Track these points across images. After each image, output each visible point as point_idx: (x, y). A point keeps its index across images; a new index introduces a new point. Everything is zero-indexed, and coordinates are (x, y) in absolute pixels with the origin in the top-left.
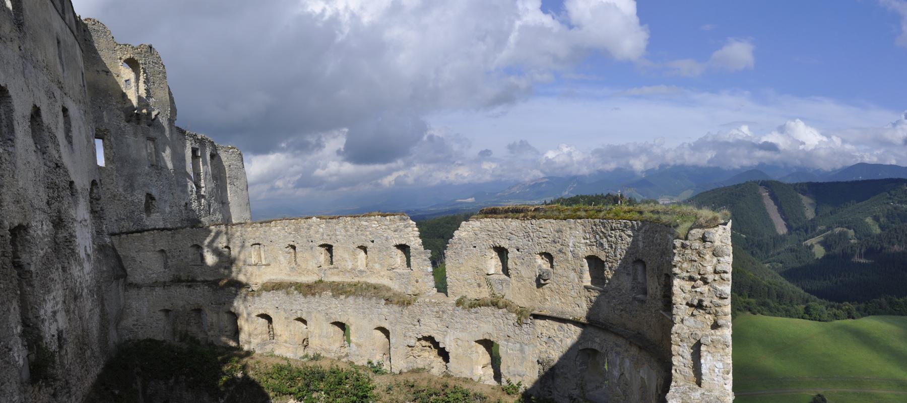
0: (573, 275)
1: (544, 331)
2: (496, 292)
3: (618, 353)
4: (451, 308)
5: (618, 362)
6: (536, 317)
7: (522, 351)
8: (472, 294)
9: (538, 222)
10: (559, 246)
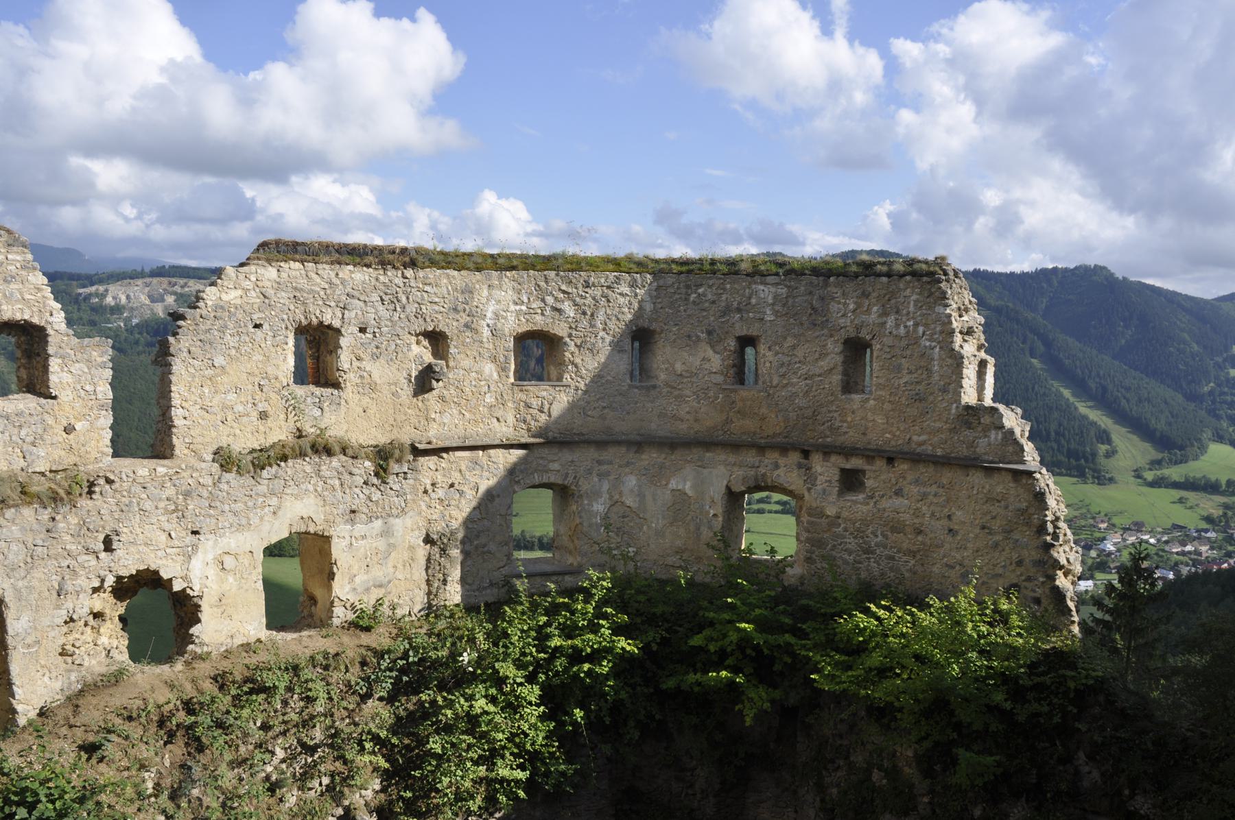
0: (489, 369)
1: (439, 478)
2: (309, 430)
4: (208, 481)
5: (606, 486)
6: (417, 452)
7: (386, 533)
8: (244, 441)
9: (421, 274)
10: (464, 318)
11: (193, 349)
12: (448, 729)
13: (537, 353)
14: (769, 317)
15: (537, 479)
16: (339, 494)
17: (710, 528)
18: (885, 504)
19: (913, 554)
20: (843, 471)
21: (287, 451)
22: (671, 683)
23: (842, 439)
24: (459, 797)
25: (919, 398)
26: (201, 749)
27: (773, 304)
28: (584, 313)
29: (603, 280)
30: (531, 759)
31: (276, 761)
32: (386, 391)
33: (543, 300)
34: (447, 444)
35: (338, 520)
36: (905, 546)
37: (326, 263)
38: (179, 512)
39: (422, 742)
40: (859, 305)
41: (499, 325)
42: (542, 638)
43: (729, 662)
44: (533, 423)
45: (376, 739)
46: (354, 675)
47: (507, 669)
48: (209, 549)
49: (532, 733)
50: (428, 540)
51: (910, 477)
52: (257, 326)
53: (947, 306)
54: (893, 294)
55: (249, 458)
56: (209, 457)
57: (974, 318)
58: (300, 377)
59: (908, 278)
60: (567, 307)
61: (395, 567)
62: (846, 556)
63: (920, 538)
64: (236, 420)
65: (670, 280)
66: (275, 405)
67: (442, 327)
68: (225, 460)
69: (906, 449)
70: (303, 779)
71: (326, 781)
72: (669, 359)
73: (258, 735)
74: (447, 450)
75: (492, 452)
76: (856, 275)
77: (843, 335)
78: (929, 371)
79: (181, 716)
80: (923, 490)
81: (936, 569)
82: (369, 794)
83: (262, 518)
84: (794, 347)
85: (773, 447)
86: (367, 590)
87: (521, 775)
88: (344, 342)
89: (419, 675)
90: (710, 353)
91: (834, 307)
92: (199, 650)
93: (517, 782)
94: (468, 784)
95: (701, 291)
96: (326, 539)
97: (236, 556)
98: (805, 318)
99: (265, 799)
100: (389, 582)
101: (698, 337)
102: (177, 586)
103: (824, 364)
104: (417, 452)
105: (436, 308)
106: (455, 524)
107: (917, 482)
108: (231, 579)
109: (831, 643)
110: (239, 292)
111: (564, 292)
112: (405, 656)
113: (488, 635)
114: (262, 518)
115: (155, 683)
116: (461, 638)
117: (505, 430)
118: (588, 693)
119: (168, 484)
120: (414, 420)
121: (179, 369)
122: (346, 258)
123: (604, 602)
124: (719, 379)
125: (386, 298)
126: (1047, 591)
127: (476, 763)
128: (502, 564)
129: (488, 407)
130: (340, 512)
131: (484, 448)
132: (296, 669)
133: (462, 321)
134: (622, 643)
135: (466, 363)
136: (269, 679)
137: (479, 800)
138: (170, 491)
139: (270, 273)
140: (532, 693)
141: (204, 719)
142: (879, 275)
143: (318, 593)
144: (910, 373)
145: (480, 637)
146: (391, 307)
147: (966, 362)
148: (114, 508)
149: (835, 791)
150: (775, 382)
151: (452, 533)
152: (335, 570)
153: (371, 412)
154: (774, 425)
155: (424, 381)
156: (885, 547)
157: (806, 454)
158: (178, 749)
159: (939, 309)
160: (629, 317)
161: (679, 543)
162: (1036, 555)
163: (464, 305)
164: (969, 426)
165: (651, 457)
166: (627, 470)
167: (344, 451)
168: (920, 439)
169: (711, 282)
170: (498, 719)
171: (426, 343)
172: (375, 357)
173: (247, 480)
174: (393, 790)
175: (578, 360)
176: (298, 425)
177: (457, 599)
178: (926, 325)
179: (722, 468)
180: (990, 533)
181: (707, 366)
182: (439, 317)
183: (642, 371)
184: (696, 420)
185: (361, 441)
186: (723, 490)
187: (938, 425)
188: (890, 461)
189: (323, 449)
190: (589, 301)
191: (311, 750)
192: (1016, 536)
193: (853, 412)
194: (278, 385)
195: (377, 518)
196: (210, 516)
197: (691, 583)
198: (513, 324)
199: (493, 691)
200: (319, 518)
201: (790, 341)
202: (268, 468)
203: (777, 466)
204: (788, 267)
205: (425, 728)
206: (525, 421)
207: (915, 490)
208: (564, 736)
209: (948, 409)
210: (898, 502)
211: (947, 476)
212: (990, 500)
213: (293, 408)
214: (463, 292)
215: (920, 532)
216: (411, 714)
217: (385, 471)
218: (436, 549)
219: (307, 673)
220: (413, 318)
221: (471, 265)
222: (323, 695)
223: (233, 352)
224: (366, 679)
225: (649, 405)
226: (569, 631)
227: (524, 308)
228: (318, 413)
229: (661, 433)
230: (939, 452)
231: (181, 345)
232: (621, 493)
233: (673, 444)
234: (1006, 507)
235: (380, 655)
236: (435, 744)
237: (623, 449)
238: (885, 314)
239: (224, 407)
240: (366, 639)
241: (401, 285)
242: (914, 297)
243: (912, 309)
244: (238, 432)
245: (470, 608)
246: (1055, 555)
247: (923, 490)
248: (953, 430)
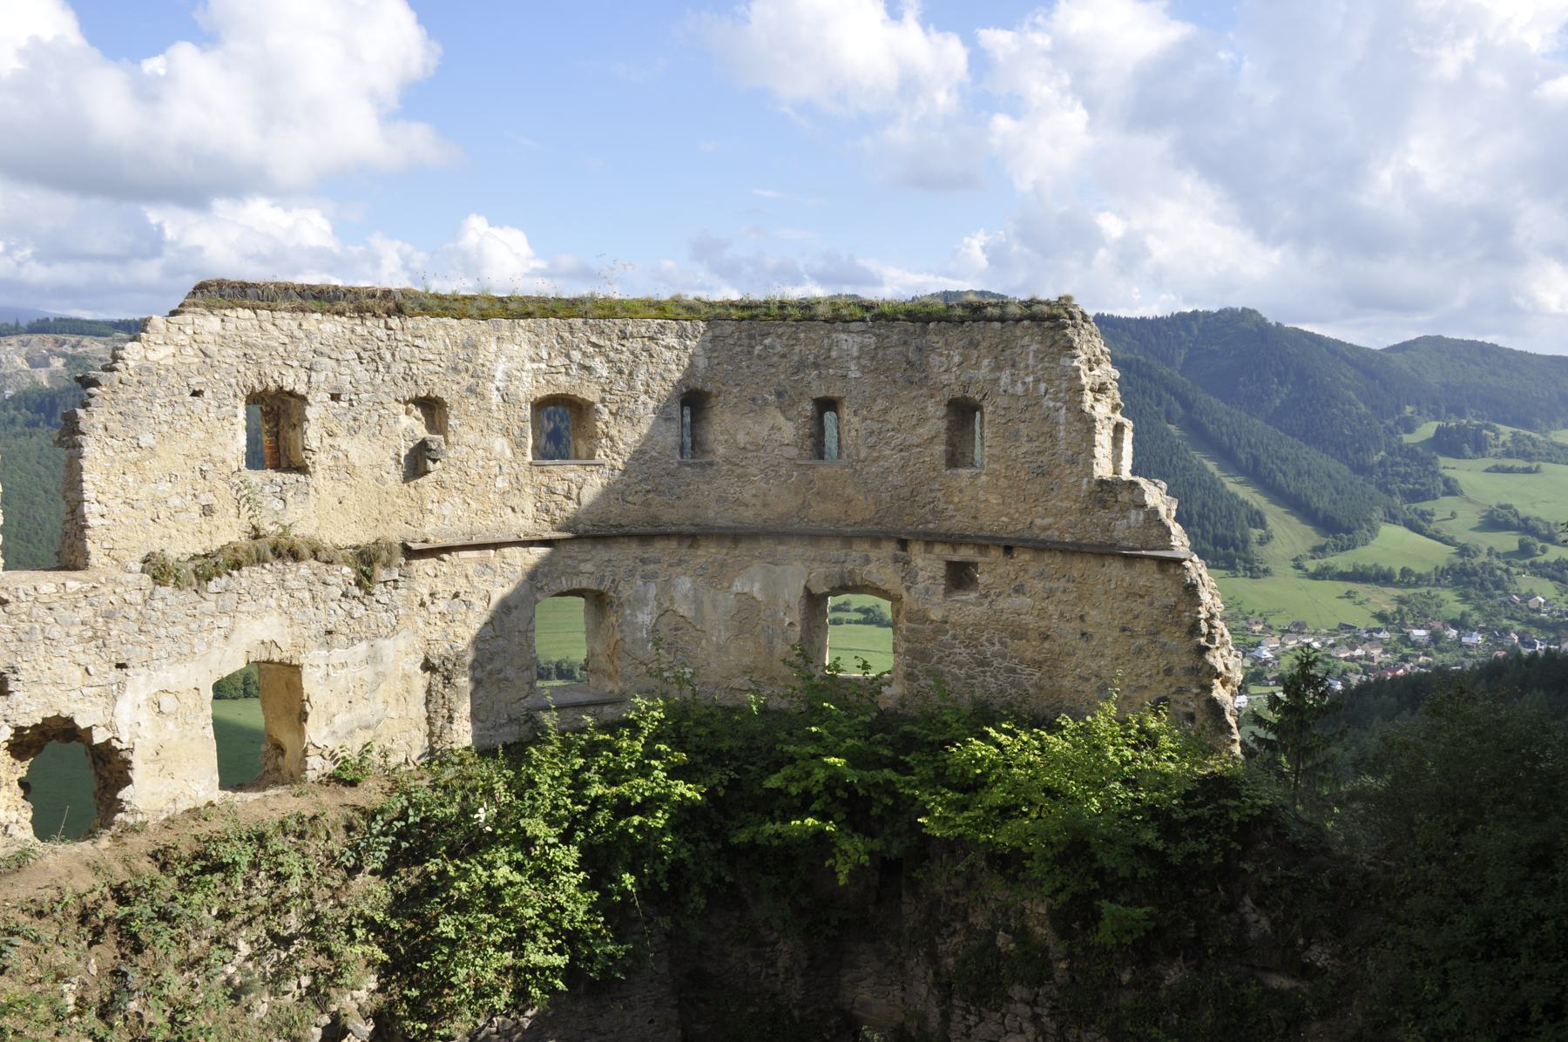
0: (501, 445)
1: (440, 586)
2: (269, 528)
4: (138, 598)
5: (652, 590)
6: (410, 553)
7: (373, 658)
8: (182, 545)
9: (410, 323)
10: (467, 380)
11: (110, 425)
12: (462, 906)
13: (561, 424)
14: (854, 373)
15: (565, 585)
16: (311, 610)
17: (786, 640)
19: (1038, 665)
20: (950, 564)
21: (241, 556)
22: (743, 837)
23: (947, 524)
24: (479, 993)
25: (1042, 472)
26: (138, 950)
27: (859, 358)
28: (620, 372)
29: (643, 330)
30: (571, 939)
31: (239, 959)
32: (367, 475)
33: (568, 356)
34: (449, 542)
35: (310, 643)
36: (1028, 655)
37: (286, 310)
38: (99, 640)
39: (429, 924)
40: (965, 358)
41: (512, 389)
42: (579, 785)
43: (815, 806)
44: (557, 513)
45: (370, 923)
46: (338, 842)
47: (536, 827)
48: (140, 686)
49: (570, 906)
50: (427, 666)
51: (1033, 569)
52: (195, 394)
53: (1074, 357)
54: (1007, 344)
55: (191, 566)
56: (138, 567)
57: (1107, 372)
58: (254, 460)
59: (1026, 323)
60: (598, 364)
61: (386, 702)
62: (956, 671)
63: (1046, 645)
64: (171, 517)
65: (728, 328)
66: (223, 498)
67: (438, 392)
68: (158, 570)
69: (1027, 535)
70: (276, 981)
71: (306, 981)
72: (728, 429)
73: (213, 927)
74: (448, 549)
75: (506, 551)
76: (962, 321)
77: (947, 394)
78: (1052, 437)
79: (110, 908)
80: (1049, 585)
81: (1066, 683)
82: (362, 995)
83: (209, 645)
84: (886, 411)
85: (861, 537)
86: (351, 733)
87: (559, 961)
88: (311, 412)
89: (422, 843)
90: (781, 419)
91: (935, 360)
92: (130, 820)
93: (554, 970)
94: (490, 975)
95: (767, 341)
96: (296, 669)
97: (177, 695)
98: (899, 375)
99: (227, 1009)
100: (379, 722)
101: (765, 400)
102: (99, 738)
103: (924, 432)
104: (410, 553)
105: (431, 367)
106: (462, 645)
107: (1041, 575)
108: (171, 726)
109: (941, 779)
110: (172, 349)
111: (594, 345)
112: (403, 815)
113: (510, 785)
114: (209, 645)
115: (73, 866)
116: (474, 790)
117: (523, 522)
118: (639, 853)
119: (83, 603)
120: (405, 513)
121: (92, 450)
122: (311, 304)
123: (657, 737)
125: (364, 355)
126: (1202, 705)
127: (500, 948)
128: (523, 694)
129: (500, 493)
130: (312, 633)
131: (496, 546)
132: (261, 838)
133: (465, 384)
134: (681, 788)
135: (471, 437)
136: (226, 853)
137: (505, 995)
138: (86, 613)
139: (212, 323)
140: (569, 855)
141: (142, 908)
142: (991, 319)
143: (287, 739)
144: (1030, 440)
145: (500, 787)
146: (372, 367)
147: (1098, 426)
148: (10, 637)
149: (951, 961)
150: (862, 456)
151: (458, 657)
152: (308, 708)
153: (348, 503)
154: (863, 508)
155: (417, 462)
156: (1004, 657)
157: (903, 544)
158: (108, 951)
159: (1065, 361)
160: (678, 375)
161: (747, 660)
162: (1188, 661)
163: (466, 363)
164: (1104, 504)
165: (708, 553)
166: (679, 570)
167: (315, 554)
168: (1044, 523)
169: (780, 331)
170: (526, 890)
171: (418, 412)
172: (352, 432)
173: (189, 595)
174: (394, 988)
175: (613, 432)
176: (254, 521)
177: (467, 740)
178: (1049, 381)
179: (798, 564)
180: (1132, 637)
181: (777, 436)
182: (435, 378)
183: (694, 445)
184: (765, 505)
185: (337, 541)
186: (801, 592)
187: (1066, 504)
188: (1008, 550)
189: (288, 552)
190: (626, 356)
191: (286, 942)
192: (1164, 638)
193: (961, 491)
194: (226, 471)
195: (361, 640)
196: (140, 643)
197: (764, 710)
198: (530, 387)
199: (518, 856)
200: (285, 642)
201: (881, 404)
202: (216, 579)
203: (867, 561)
204: (876, 311)
205: (432, 907)
206: (547, 511)
207: (1039, 585)
208: (613, 911)
209: (1077, 485)
210: (1019, 601)
211: (1078, 566)
212: (1132, 595)
213: (246, 499)
214: (464, 347)
216: (415, 888)
217: (369, 578)
218: (438, 678)
219: (277, 843)
220: (400, 381)
221: (474, 312)
222: (298, 871)
223: (165, 428)
224: (354, 848)
225: (705, 487)
226: (612, 776)
227: (543, 366)
228: (281, 505)
229: (721, 522)
230: (1068, 538)
231: (94, 419)
232: (672, 600)
233: (735, 536)
234: (1151, 604)
235: (371, 816)
236: (447, 927)
237: (673, 544)
239: (155, 501)
240: (351, 796)
241: (385, 338)
242: (1034, 347)
243: (1031, 361)
244: (174, 532)
245: (485, 752)
246: (1211, 660)
247: (1049, 585)
248: (1084, 511)
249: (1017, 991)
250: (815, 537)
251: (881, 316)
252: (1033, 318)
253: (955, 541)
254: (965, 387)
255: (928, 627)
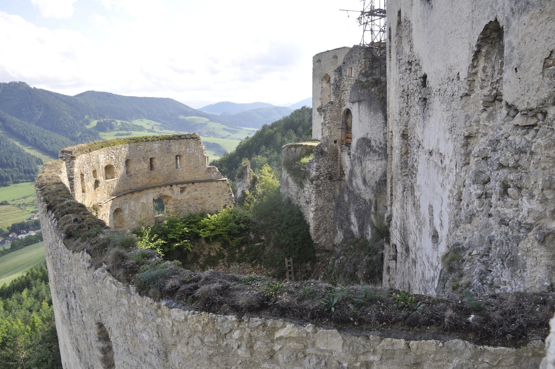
3: (127, 203)
18: (193, 194)
20: (181, 188)
40: (179, 147)
51: (198, 186)
54: (188, 143)
60: (113, 156)
72: (135, 167)
77: (176, 154)
91: (172, 147)
103: (171, 162)
124: (147, 170)
142: (184, 139)
149: (201, 263)
154: (161, 180)
157: (171, 186)
165: (136, 195)
168: (198, 177)
188: (193, 183)
192: (224, 194)
198: (104, 165)
201: (163, 158)
203: (164, 190)
207: (200, 189)
210: (196, 192)
211: (207, 184)
215: (202, 198)
229: (134, 188)
233: (140, 190)
238: (186, 148)
248: (205, 174)
249: (220, 261)
250: (154, 188)
251: (161, 139)
252: (193, 138)
253: (182, 183)
254: (179, 153)
255: (178, 202)
